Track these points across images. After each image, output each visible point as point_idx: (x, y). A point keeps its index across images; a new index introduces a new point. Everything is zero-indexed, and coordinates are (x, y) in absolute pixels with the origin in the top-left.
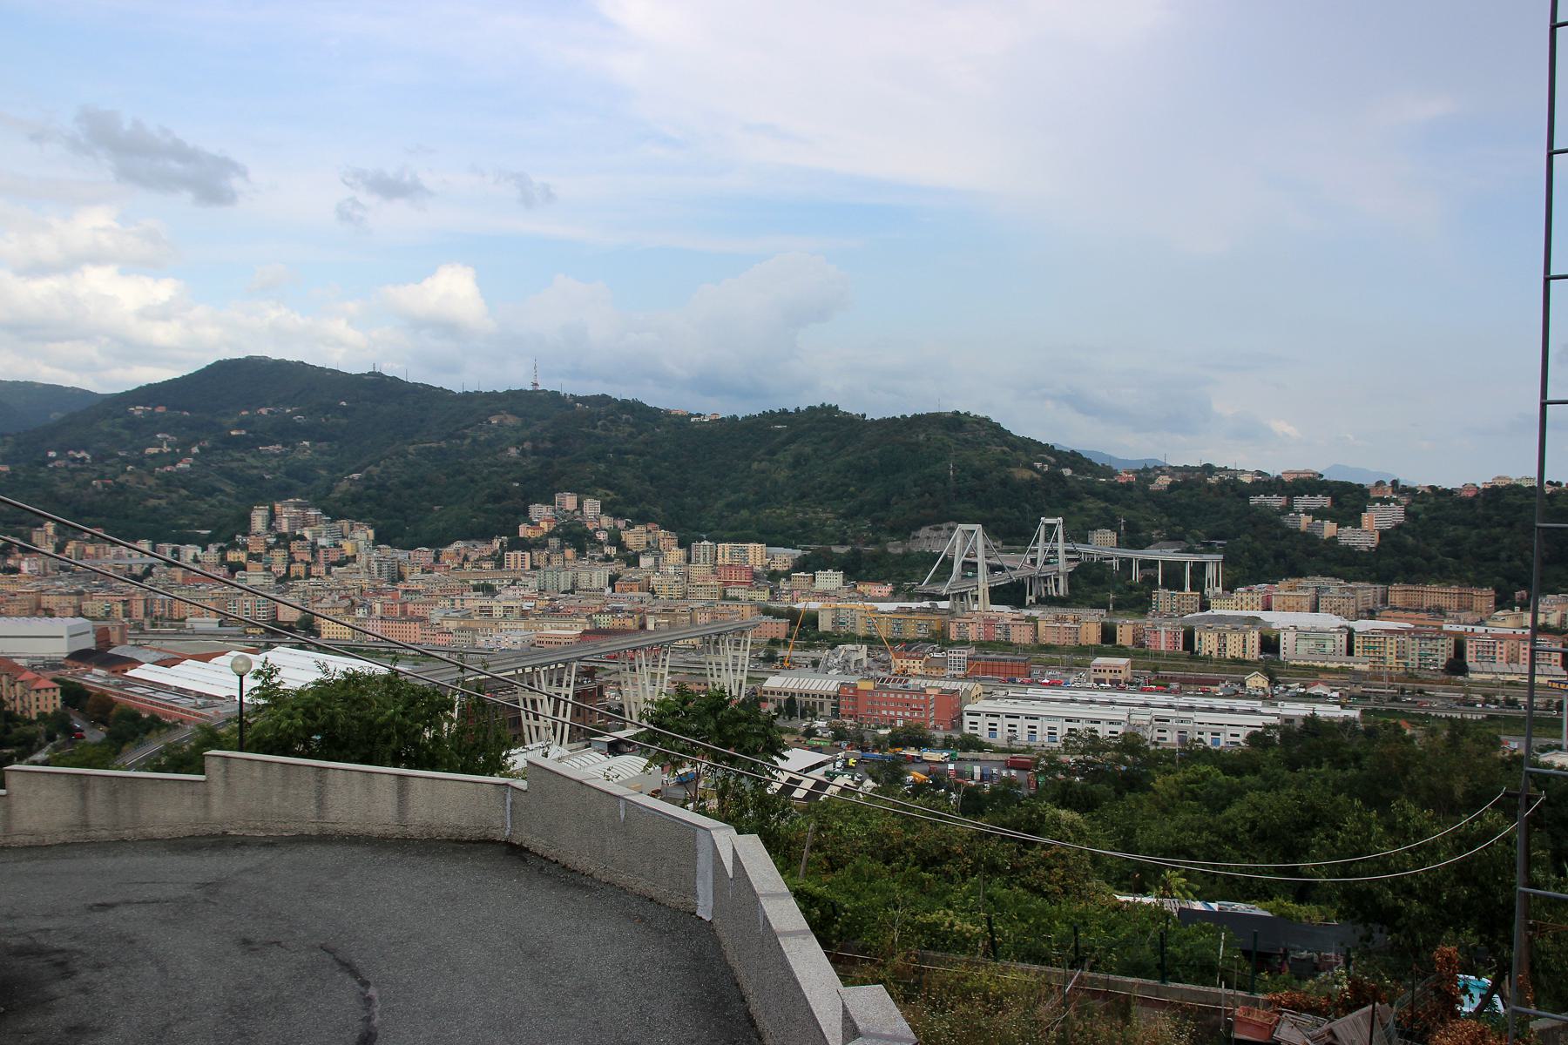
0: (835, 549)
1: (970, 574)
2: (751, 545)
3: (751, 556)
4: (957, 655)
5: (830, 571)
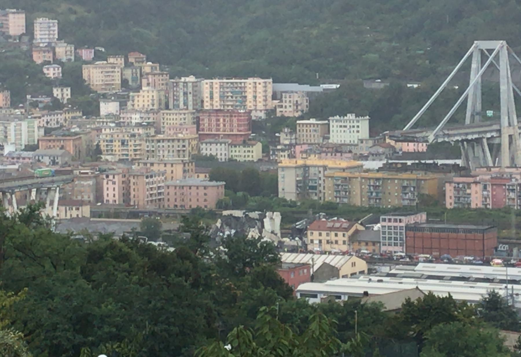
0: (367, 85)
1: (490, 113)
2: (250, 80)
3: (250, 97)
4: (392, 224)
5: (351, 116)
